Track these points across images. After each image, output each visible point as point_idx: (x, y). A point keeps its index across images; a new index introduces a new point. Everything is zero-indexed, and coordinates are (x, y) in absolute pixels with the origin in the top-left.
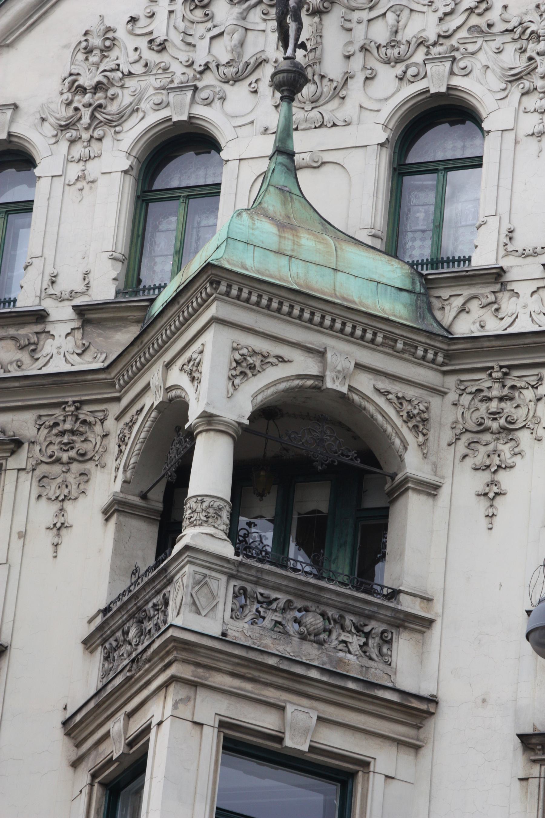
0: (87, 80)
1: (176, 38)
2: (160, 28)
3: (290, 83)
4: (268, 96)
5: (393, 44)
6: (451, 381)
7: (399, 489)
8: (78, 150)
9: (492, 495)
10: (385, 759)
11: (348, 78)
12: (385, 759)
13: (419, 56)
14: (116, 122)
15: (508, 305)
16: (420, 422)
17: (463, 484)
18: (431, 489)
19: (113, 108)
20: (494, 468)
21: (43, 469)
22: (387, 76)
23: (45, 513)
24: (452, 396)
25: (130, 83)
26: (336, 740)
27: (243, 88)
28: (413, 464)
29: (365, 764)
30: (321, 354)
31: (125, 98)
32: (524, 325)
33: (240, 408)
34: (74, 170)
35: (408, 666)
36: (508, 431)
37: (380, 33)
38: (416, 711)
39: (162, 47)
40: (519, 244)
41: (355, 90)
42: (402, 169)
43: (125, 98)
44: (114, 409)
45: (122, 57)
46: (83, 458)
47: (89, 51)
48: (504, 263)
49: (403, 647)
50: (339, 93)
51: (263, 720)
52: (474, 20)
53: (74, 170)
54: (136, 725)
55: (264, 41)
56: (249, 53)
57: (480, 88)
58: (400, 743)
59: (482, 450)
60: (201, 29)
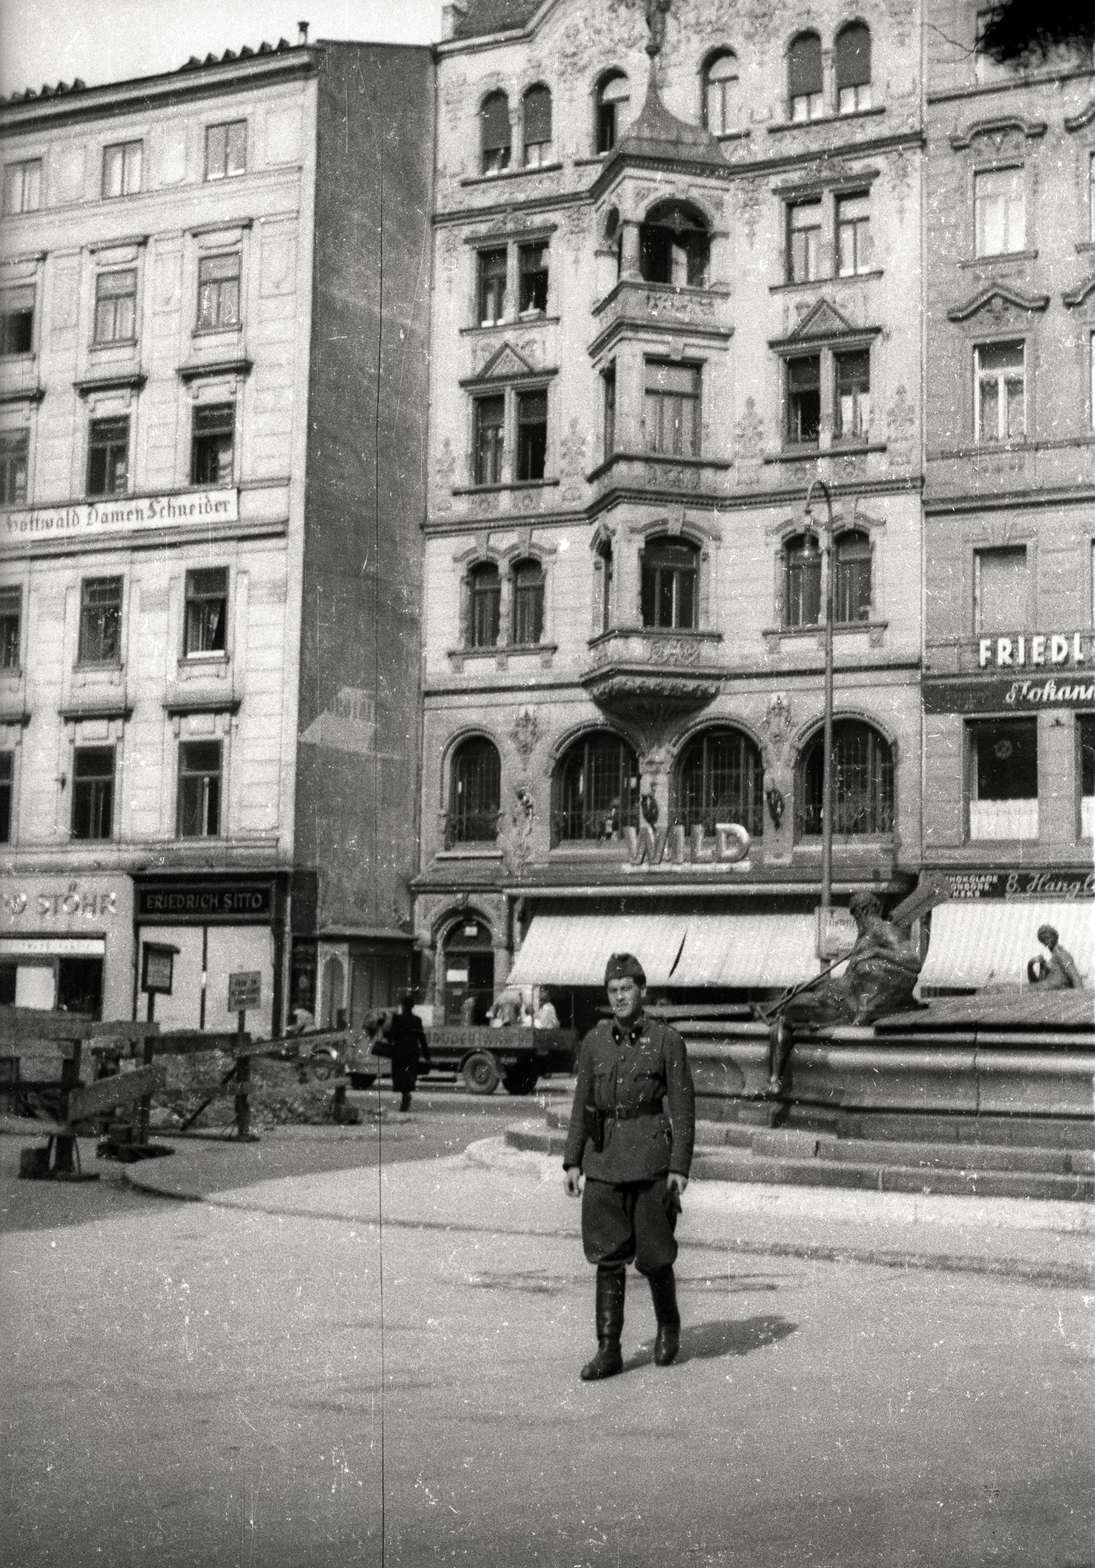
0: (570, 50)
1: (604, 27)
2: (597, 23)
3: (653, 51)
4: (645, 56)
5: (698, 24)
6: (732, 186)
7: (714, 236)
8: (568, 85)
9: (752, 235)
11: (679, 41)
13: (709, 29)
15: (754, 147)
16: (719, 205)
19: (581, 63)
20: (751, 223)
21: (569, 236)
22: (695, 38)
24: (732, 192)
25: (588, 51)
26: (691, 353)
27: (634, 49)
29: (705, 360)
31: (586, 58)
32: (761, 157)
33: (640, 215)
34: (567, 95)
35: (723, 314)
37: (691, 18)
39: (598, 32)
40: (757, 117)
41: (683, 48)
42: (706, 82)
43: (586, 58)
44: (593, 208)
45: (584, 37)
46: (583, 231)
47: (568, 37)
48: (751, 126)
50: (675, 49)
51: (661, 349)
52: (731, 10)
53: (567, 95)
54: (610, 356)
55: (641, 27)
56: (636, 33)
57: (735, 42)
58: (720, 349)
59: (747, 215)
60: (615, 23)
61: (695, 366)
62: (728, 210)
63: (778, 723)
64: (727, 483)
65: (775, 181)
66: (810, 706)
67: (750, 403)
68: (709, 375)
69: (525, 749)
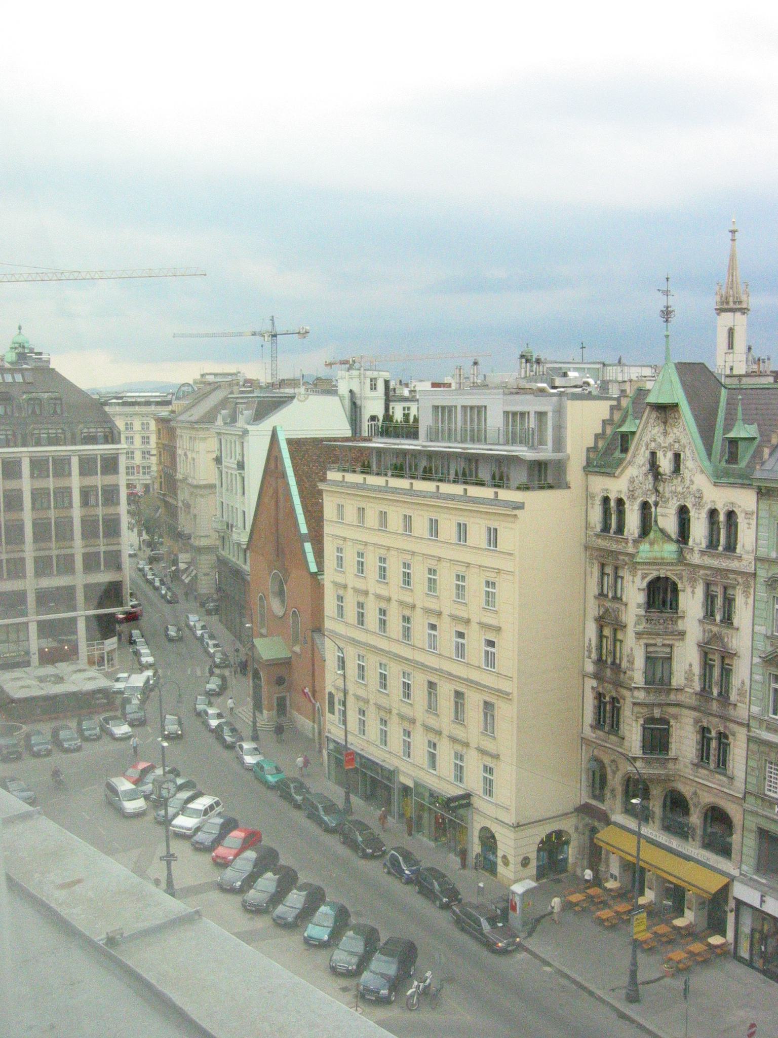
0: (631, 489)
9: (693, 592)
10: (677, 644)
12: (677, 644)
14: (635, 499)
16: (681, 578)
17: (689, 590)
18: (683, 591)
23: (631, 578)
28: (680, 586)
30: (658, 570)
35: (681, 625)
36: (695, 581)
38: (682, 634)
49: (680, 622)
51: (652, 642)
61: (671, 646)
62: (685, 579)
63: (695, 800)
64: (681, 698)
65: (702, 572)
66: (707, 799)
67: (691, 665)
68: (675, 649)
69: (614, 773)
